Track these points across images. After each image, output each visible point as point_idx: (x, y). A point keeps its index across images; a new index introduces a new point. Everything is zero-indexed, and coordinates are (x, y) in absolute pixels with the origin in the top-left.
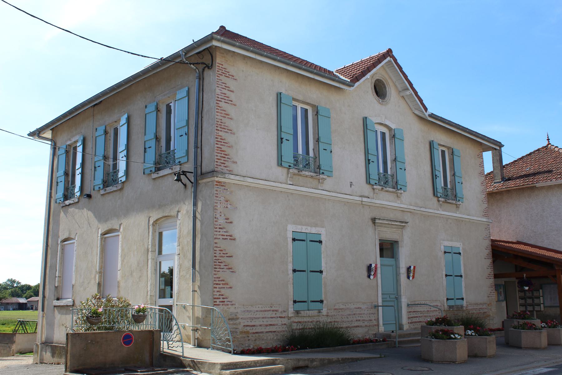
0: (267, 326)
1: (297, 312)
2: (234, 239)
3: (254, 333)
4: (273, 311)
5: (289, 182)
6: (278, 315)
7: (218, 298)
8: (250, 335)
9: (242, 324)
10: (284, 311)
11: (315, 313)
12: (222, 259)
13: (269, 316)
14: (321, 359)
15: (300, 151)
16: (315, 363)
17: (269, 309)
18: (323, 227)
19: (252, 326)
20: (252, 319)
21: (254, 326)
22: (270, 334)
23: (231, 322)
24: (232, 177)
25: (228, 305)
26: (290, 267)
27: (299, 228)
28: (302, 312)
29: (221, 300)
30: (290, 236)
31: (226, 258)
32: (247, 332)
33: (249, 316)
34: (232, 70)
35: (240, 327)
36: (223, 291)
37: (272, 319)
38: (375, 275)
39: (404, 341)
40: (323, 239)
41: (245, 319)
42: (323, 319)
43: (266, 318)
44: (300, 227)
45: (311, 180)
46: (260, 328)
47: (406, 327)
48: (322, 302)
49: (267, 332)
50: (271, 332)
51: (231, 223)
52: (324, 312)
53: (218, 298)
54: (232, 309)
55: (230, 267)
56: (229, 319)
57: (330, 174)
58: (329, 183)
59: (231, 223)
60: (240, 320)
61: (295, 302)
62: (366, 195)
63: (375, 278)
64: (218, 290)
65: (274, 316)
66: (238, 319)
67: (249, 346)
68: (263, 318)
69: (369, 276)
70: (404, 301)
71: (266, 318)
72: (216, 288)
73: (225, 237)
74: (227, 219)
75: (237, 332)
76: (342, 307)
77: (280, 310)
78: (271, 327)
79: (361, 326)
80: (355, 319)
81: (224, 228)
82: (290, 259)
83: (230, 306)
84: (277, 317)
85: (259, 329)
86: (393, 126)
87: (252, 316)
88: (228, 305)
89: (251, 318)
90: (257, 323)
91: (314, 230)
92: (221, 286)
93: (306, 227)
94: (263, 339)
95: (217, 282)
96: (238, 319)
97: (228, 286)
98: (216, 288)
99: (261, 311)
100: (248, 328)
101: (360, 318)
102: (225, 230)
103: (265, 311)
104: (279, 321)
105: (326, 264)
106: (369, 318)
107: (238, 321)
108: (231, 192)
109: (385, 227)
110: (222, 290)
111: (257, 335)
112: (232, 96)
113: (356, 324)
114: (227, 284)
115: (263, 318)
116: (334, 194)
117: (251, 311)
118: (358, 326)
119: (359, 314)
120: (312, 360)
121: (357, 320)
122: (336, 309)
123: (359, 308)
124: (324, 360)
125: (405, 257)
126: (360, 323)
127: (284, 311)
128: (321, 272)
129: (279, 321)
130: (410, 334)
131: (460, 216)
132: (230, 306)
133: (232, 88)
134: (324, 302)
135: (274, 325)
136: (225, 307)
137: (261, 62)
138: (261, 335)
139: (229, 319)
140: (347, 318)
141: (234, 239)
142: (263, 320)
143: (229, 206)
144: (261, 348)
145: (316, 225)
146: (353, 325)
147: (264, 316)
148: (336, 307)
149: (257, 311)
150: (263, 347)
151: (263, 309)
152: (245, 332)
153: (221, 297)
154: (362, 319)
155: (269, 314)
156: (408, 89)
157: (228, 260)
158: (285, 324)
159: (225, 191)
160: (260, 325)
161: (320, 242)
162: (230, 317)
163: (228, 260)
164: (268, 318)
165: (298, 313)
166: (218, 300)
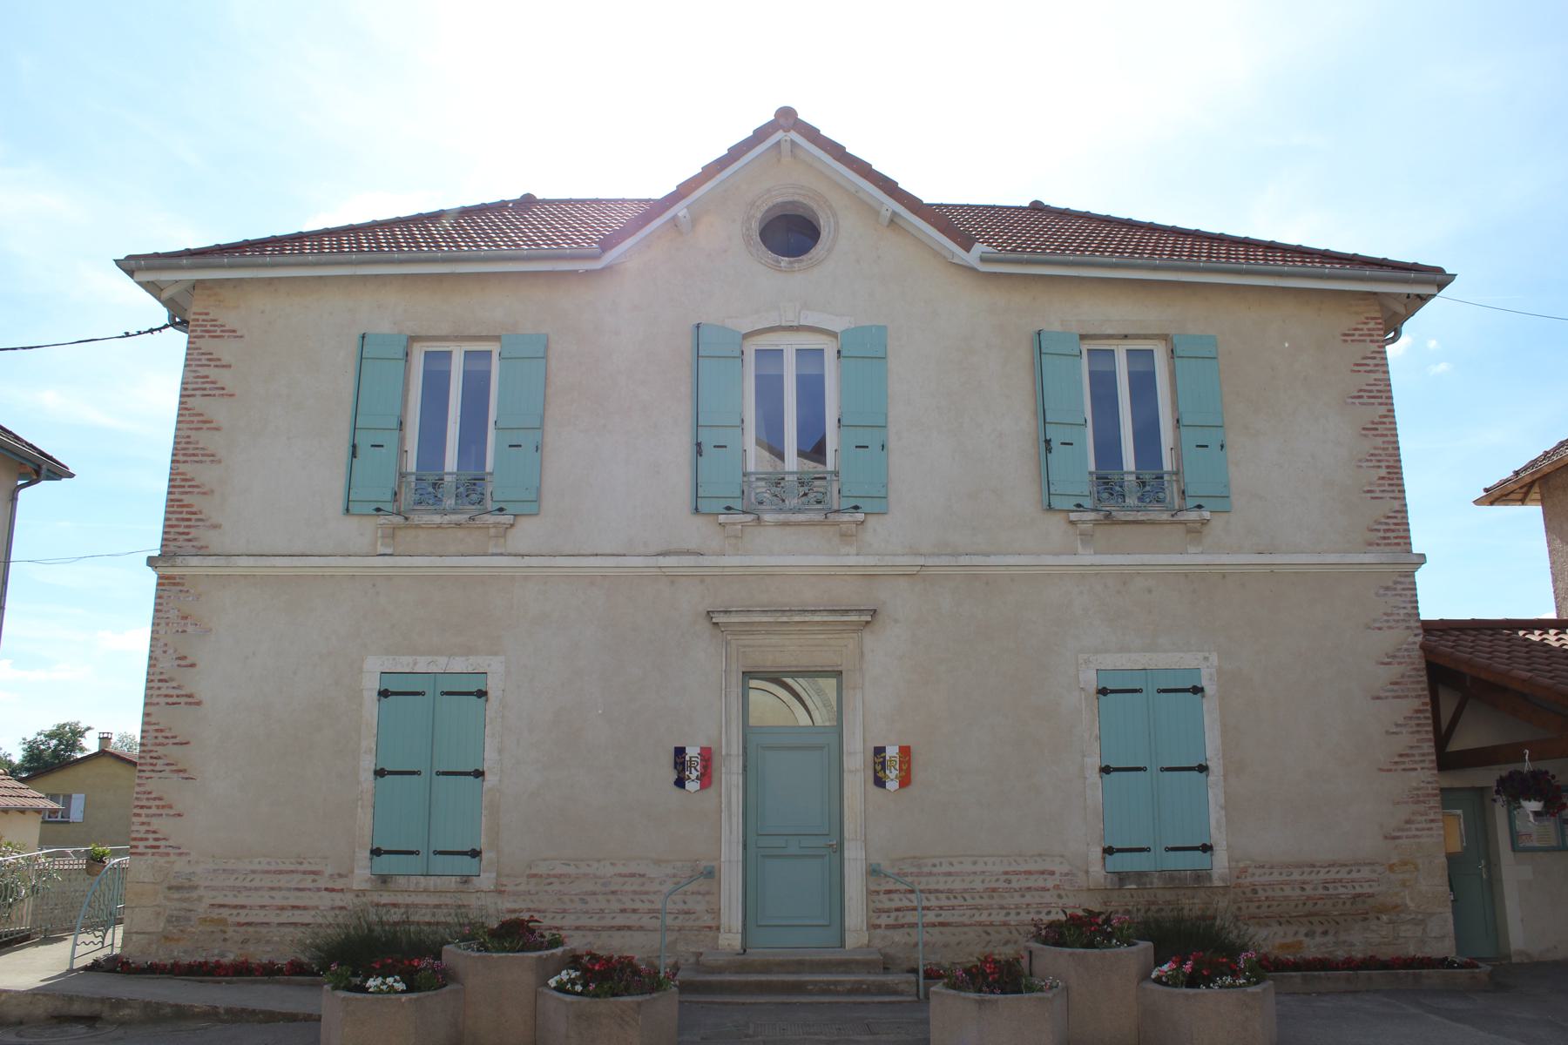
0: (282, 908)
1: (384, 880)
2: (198, 704)
3: (239, 924)
4: (304, 873)
5: (381, 550)
6: (322, 883)
7: (141, 839)
8: (230, 931)
9: (207, 901)
10: (340, 876)
11: (452, 883)
12: (161, 750)
13: (293, 885)
14: (147, 1005)
15: (451, 462)
16: (127, 1011)
17: (292, 868)
18: (496, 654)
19: (235, 907)
20: (238, 890)
21: (243, 907)
22: (291, 929)
23: (176, 896)
24: (194, 561)
25: (168, 854)
26: (368, 764)
27: (404, 663)
28: (402, 880)
29: (151, 843)
30: (372, 684)
31: (171, 747)
32: (223, 922)
33: (231, 882)
34: (230, 319)
35: (202, 909)
36: (156, 823)
37: (300, 894)
38: (706, 779)
39: (721, 983)
40: (494, 686)
41: (214, 889)
42: (473, 901)
43: (280, 889)
45: (460, 533)
46: (262, 913)
47: (851, 941)
48: (475, 854)
49: (280, 924)
50: (295, 924)
51: (193, 665)
52: (486, 880)
53: (141, 839)
54: (180, 865)
55: (180, 767)
56: (170, 888)
57: (533, 504)
58: (527, 533)
59: (193, 665)
60: (201, 892)
61: (376, 852)
62: (692, 546)
63: (711, 791)
64: (143, 819)
65: (308, 884)
66: (195, 888)
67: (223, 956)
68: (272, 889)
69: (680, 783)
70: (855, 856)
71: (280, 889)
72: (139, 815)
73: (175, 700)
74: (184, 658)
75: (188, 919)
76: (571, 870)
77: (329, 871)
78: (297, 912)
79: (641, 928)
80: (616, 906)
81: (172, 680)
82: (369, 742)
83: (173, 858)
84: (319, 890)
85: (259, 916)
86: (838, 325)
87: (238, 883)
88: (168, 854)
89: (233, 888)
90: (255, 899)
91: (459, 665)
92: (154, 811)
93: (430, 658)
94: (268, 942)
95: (144, 803)
96: (195, 888)
97: (172, 812)
98: (139, 815)
99: (267, 872)
100: (225, 912)
101: (638, 905)
102: (174, 684)
103: (281, 872)
104: (326, 900)
105: (500, 751)
106: (681, 906)
107: (194, 895)
108: (198, 597)
109: (768, 633)
110: (154, 820)
111: (250, 929)
112: (224, 377)
113: (620, 920)
114: (170, 807)
115: (272, 889)
116: (534, 561)
117: (233, 871)
118: (629, 928)
119: (635, 892)
120: (118, 1004)
121: (623, 911)
122: (535, 876)
123: (633, 875)
124: (159, 1006)
126: (646, 921)
127: (340, 876)
128: (479, 774)
129: (326, 900)
130: (801, 963)
131: (1201, 559)
132: (173, 858)
133: (226, 360)
134: (484, 855)
135: (305, 908)
136: (162, 861)
137: (271, 280)
138: (264, 930)
139: (170, 888)
140: (583, 901)
141: (198, 704)
142: (273, 893)
143: (190, 629)
144: (272, 964)
145: (469, 651)
146: (608, 922)
147: (276, 884)
148: (534, 871)
149: (254, 872)
150: (254, 961)
151: (272, 868)
152: (212, 921)
153: (151, 836)
154: (647, 906)
155: (294, 881)
156: (675, 218)
157: (172, 751)
158: (342, 908)
159: (182, 595)
160: (262, 907)
161: (482, 694)
162: (174, 883)
163: (172, 751)
164: (289, 889)
165: (384, 882)
166: (141, 844)
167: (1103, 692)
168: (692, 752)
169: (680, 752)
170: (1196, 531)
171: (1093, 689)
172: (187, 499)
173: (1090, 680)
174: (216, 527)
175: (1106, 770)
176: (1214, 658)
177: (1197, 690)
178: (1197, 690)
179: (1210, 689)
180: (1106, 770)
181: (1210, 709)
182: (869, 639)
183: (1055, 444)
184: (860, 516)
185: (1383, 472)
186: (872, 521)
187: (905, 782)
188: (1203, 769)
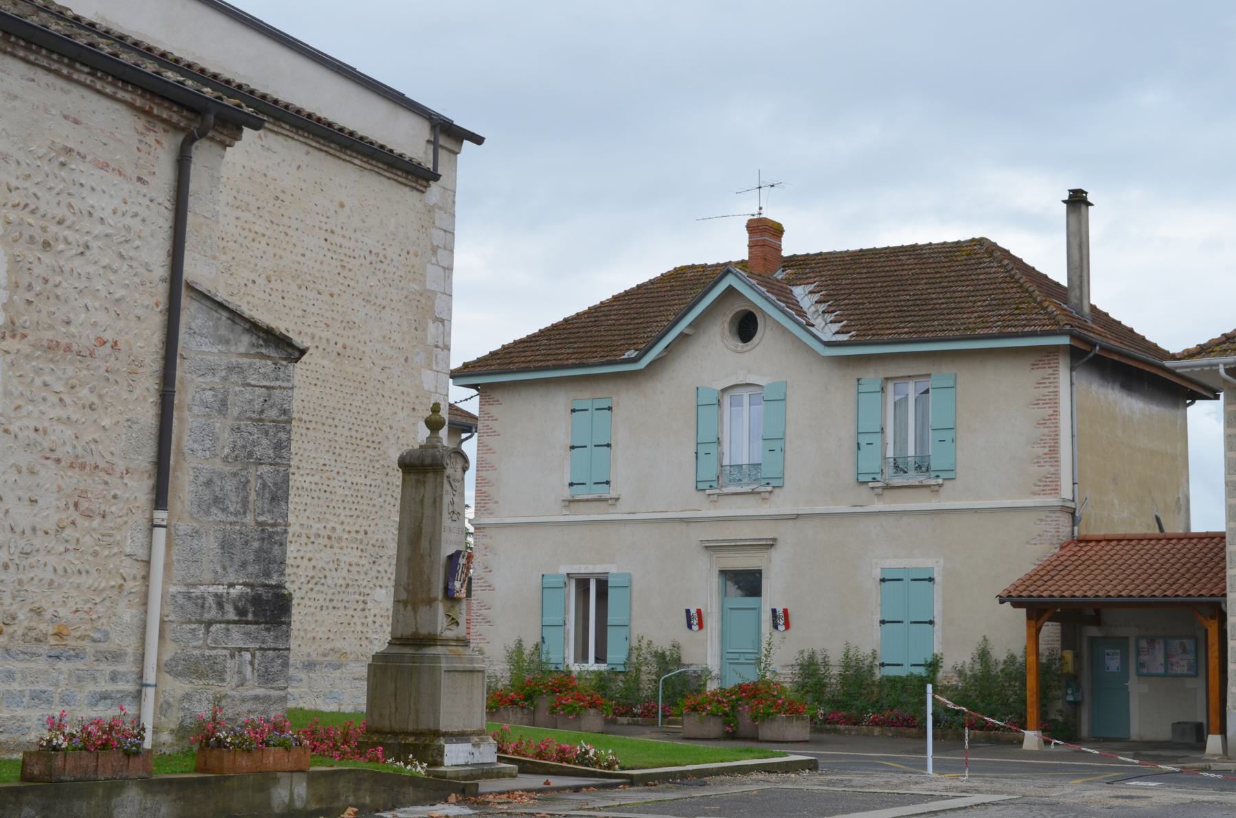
44: (576, 567)
125: (773, 595)
167: (883, 580)
168: (693, 611)
169: (688, 611)
170: (935, 489)
171: (879, 577)
172: (484, 489)
173: (878, 574)
174: (496, 502)
175: (883, 622)
176: (941, 562)
177: (931, 580)
178: (931, 580)
179: (938, 578)
180: (883, 622)
181: (937, 588)
182: (774, 554)
183: (863, 446)
184: (769, 489)
185: (1046, 450)
186: (777, 491)
187: (787, 625)
188: (931, 622)
